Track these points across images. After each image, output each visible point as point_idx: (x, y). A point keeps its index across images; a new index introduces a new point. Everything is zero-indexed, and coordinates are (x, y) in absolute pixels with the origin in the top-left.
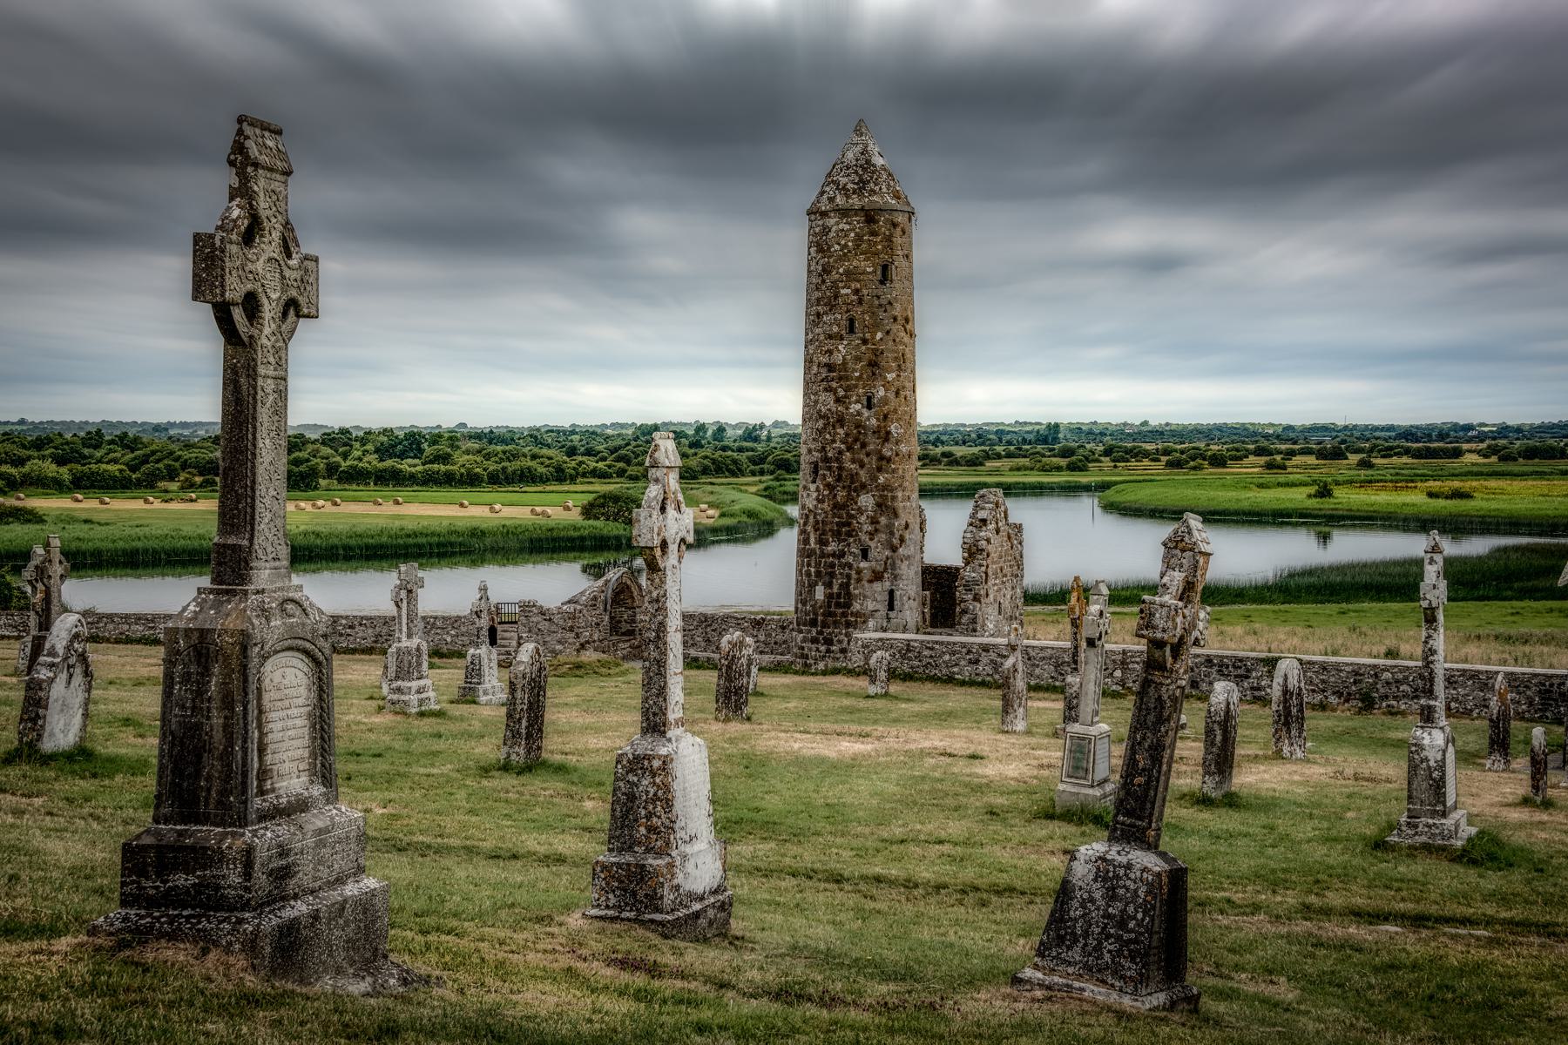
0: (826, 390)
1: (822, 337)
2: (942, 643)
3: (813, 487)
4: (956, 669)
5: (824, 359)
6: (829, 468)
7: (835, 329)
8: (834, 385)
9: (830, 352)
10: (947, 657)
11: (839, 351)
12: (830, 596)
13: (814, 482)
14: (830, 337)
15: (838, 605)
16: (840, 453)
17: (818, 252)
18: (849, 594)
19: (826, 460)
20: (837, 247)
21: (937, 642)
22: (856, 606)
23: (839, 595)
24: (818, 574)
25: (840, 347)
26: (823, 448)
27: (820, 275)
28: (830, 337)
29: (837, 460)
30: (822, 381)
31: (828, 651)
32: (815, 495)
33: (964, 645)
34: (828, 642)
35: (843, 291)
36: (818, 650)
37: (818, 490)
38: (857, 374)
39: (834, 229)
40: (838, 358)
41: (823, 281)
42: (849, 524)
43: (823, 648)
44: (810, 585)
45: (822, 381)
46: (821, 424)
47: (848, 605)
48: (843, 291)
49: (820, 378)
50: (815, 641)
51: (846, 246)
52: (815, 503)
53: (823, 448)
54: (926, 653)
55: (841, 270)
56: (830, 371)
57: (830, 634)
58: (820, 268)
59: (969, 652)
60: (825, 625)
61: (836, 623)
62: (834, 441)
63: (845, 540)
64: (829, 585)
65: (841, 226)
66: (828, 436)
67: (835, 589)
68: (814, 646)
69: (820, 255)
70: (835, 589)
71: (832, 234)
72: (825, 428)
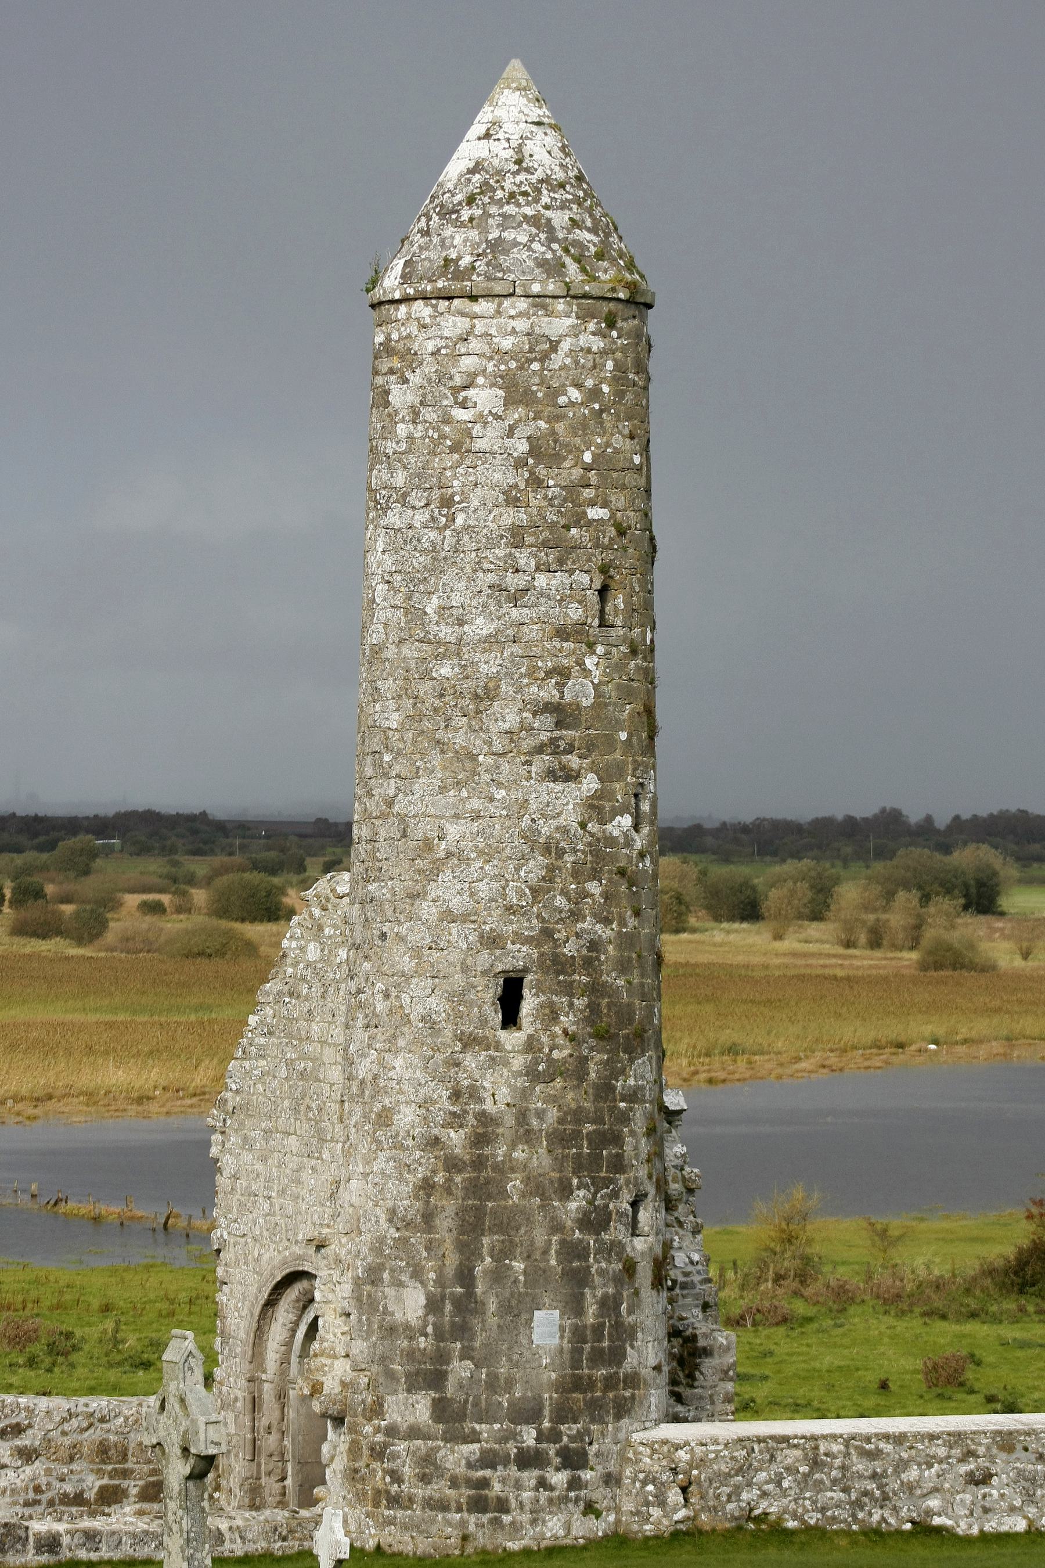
0: (552, 775)
1: (532, 632)
2: (899, 1439)
3: (512, 1039)
4: (934, 1503)
5: (548, 692)
6: (568, 989)
7: (575, 613)
8: (574, 761)
9: (562, 674)
10: (912, 1474)
11: (586, 673)
12: (578, 1335)
14: (562, 633)
15: (598, 1357)
16: (595, 946)
17: (509, 402)
18: (618, 1325)
19: (558, 965)
20: (575, 394)
21: (886, 1437)
22: (631, 1360)
23: (598, 1330)
24: (536, 1275)
25: (590, 662)
28: (562, 633)
29: (589, 963)
30: (540, 750)
31: (575, 1484)
32: (518, 1062)
33: (957, 1438)
35: (595, 513)
36: (543, 1483)
37: (531, 1045)
38: (623, 736)
39: (565, 346)
42: (617, 1140)
43: (559, 1478)
44: (506, 1308)
45: (540, 750)
46: (534, 868)
47: (617, 1356)
48: (595, 513)
49: (527, 744)
50: (527, 1460)
51: (595, 394)
52: (521, 1082)
53: (547, 933)
54: (860, 1466)
55: (587, 457)
56: (559, 725)
57: (579, 1436)
58: (523, 447)
59: (970, 1454)
60: (562, 1414)
61: (596, 1410)
62: (576, 915)
63: (607, 1182)
64: (574, 1306)
65: (585, 340)
66: (560, 901)
67: (591, 1315)
68: (530, 1477)
69: (517, 413)
70: (591, 1315)
71: (558, 359)
72: (549, 878)
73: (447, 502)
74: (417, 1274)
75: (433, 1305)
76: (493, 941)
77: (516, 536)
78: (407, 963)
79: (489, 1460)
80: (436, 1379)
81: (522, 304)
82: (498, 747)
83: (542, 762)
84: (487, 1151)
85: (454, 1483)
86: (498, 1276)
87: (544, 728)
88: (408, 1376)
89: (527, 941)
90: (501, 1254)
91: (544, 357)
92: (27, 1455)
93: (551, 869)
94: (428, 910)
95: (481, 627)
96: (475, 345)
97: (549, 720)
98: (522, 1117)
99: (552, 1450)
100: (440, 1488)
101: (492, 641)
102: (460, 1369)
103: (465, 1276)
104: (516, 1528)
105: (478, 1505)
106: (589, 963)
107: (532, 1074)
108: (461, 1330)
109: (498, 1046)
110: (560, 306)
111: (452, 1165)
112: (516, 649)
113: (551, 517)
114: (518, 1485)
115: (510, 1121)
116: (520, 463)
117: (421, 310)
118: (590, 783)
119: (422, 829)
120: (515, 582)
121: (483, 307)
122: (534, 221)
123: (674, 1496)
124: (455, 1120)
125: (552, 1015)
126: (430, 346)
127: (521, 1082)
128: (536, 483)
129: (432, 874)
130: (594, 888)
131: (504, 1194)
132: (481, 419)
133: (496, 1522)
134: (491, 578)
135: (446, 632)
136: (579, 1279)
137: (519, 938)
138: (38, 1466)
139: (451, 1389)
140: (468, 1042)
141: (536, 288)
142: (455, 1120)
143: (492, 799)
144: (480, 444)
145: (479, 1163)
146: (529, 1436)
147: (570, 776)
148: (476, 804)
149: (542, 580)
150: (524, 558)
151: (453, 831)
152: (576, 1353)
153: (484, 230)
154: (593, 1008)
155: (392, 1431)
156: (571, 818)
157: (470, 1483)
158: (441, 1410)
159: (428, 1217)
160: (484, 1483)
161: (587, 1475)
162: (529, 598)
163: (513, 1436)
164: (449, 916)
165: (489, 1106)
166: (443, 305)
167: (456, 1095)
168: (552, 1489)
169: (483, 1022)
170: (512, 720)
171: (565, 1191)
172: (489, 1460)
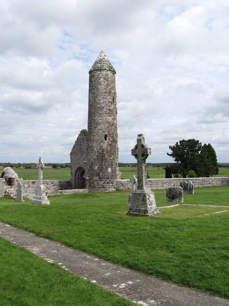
1: (107, 102)
5: (108, 108)
7: (111, 100)
9: (110, 106)
13: (106, 140)
15: (114, 173)
16: (113, 133)
19: (110, 134)
24: (109, 165)
26: (109, 131)
27: (106, 86)
28: (110, 102)
31: (112, 185)
32: (107, 144)
34: (112, 183)
36: (109, 185)
37: (108, 142)
39: (109, 75)
40: (112, 108)
41: (107, 88)
43: (111, 185)
46: (107, 125)
48: (112, 91)
49: (107, 113)
50: (108, 183)
52: (107, 145)
53: (109, 131)
55: (112, 86)
56: (110, 111)
57: (113, 181)
62: (111, 130)
64: (112, 168)
66: (110, 128)
68: (108, 185)
69: (105, 81)
71: (109, 76)
73: (98, 89)
74: (97, 165)
75: (98, 168)
76: (104, 132)
77: (106, 93)
78: (95, 134)
79: (104, 183)
80: (99, 175)
81: (106, 71)
82: (104, 113)
83: (108, 115)
84: (104, 152)
85: (101, 185)
86: (105, 165)
87: (108, 112)
88: (96, 175)
89: (107, 132)
90: (105, 162)
91: (108, 76)
92: (54, 185)
93: (109, 125)
94: (97, 129)
95: (102, 101)
96: (101, 74)
97: (109, 110)
98: (107, 149)
99: (110, 182)
100: (99, 186)
101: (103, 103)
102: (101, 174)
103: (102, 165)
104: (107, 190)
105: (103, 187)
106: (113, 134)
107: (108, 145)
108: (101, 170)
109: (104, 142)
110: (109, 71)
111: (100, 154)
112: (105, 103)
113: (109, 91)
114: (107, 186)
115: (106, 149)
116: (106, 86)
117: (95, 71)
118: (112, 117)
119: (97, 121)
120: (105, 97)
121: (102, 71)
122: (106, 63)
123: (122, 186)
124: (100, 149)
125: (109, 139)
126: (96, 75)
127: (107, 145)
128: (107, 88)
129: (98, 125)
130: (113, 127)
131: (105, 157)
132: (102, 81)
133: (105, 189)
134: (103, 97)
135: (99, 102)
136: (112, 165)
137: (106, 131)
138: (55, 187)
139: (100, 176)
140: (102, 142)
141: (107, 69)
142: (100, 149)
143: (103, 118)
144: (102, 84)
145: (103, 153)
146: (108, 180)
147: (110, 116)
148: (102, 118)
149: (108, 97)
150: (106, 95)
151: (100, 121)
152: (112, 172)
153: (101, 64)
154: (113, 139)
155: (94, 181)
156: (111, 120)
157: (102, 185)
158: (100, 178)
159: (98, 159)
160: (104, 185)
161: (113, 184)
162: (107, 99)
163: (107, 181)
164: (99, 129)
165: (104, 148)
166: (98, 71)
167: (100, 147)
168: (110, 186)
169: (103, 140)
170: (105, 110)
171: (111, 157)
172: (104, 183)
